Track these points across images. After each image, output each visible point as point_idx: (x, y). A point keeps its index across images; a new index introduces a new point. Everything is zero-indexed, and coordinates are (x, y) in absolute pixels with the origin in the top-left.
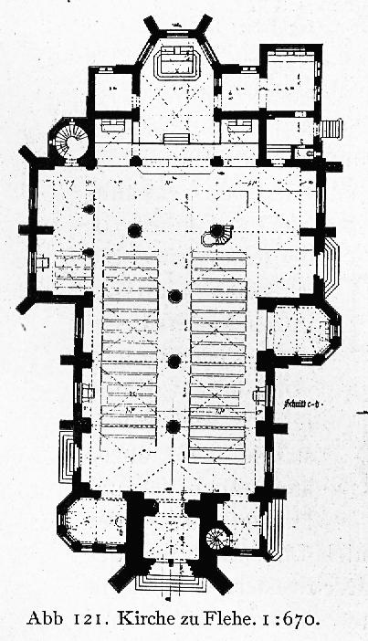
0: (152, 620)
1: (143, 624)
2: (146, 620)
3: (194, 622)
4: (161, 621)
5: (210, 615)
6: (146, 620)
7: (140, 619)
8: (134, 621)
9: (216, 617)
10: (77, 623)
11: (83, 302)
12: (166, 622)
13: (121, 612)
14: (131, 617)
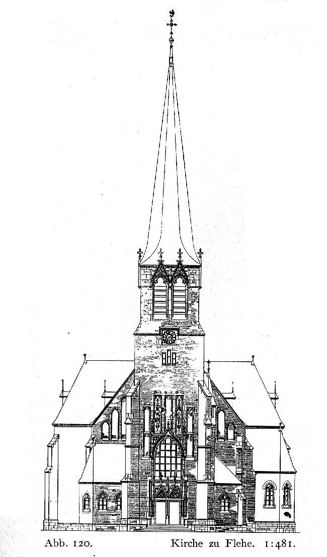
0: (190, 544)
1: (185, 546)
2: (187, 544)
3: (216, 545)
4: (195, 545)
5: (229, 541)
6: (187, 544)
7: (184, 544)
8: (180, 544)
9: (233, 543)
10: (267, 546)
11: (280, 427)
12: (198, 545)
13: (173, 540)
14: (179, 543)
